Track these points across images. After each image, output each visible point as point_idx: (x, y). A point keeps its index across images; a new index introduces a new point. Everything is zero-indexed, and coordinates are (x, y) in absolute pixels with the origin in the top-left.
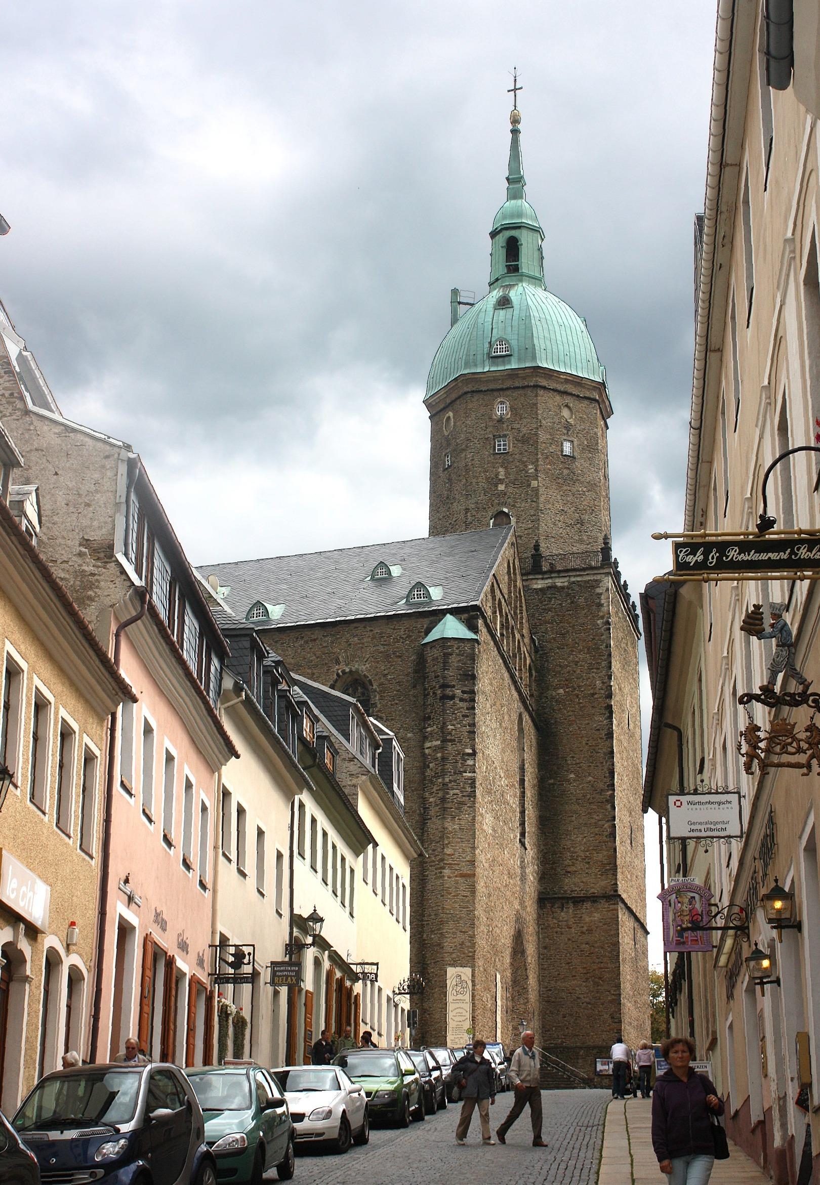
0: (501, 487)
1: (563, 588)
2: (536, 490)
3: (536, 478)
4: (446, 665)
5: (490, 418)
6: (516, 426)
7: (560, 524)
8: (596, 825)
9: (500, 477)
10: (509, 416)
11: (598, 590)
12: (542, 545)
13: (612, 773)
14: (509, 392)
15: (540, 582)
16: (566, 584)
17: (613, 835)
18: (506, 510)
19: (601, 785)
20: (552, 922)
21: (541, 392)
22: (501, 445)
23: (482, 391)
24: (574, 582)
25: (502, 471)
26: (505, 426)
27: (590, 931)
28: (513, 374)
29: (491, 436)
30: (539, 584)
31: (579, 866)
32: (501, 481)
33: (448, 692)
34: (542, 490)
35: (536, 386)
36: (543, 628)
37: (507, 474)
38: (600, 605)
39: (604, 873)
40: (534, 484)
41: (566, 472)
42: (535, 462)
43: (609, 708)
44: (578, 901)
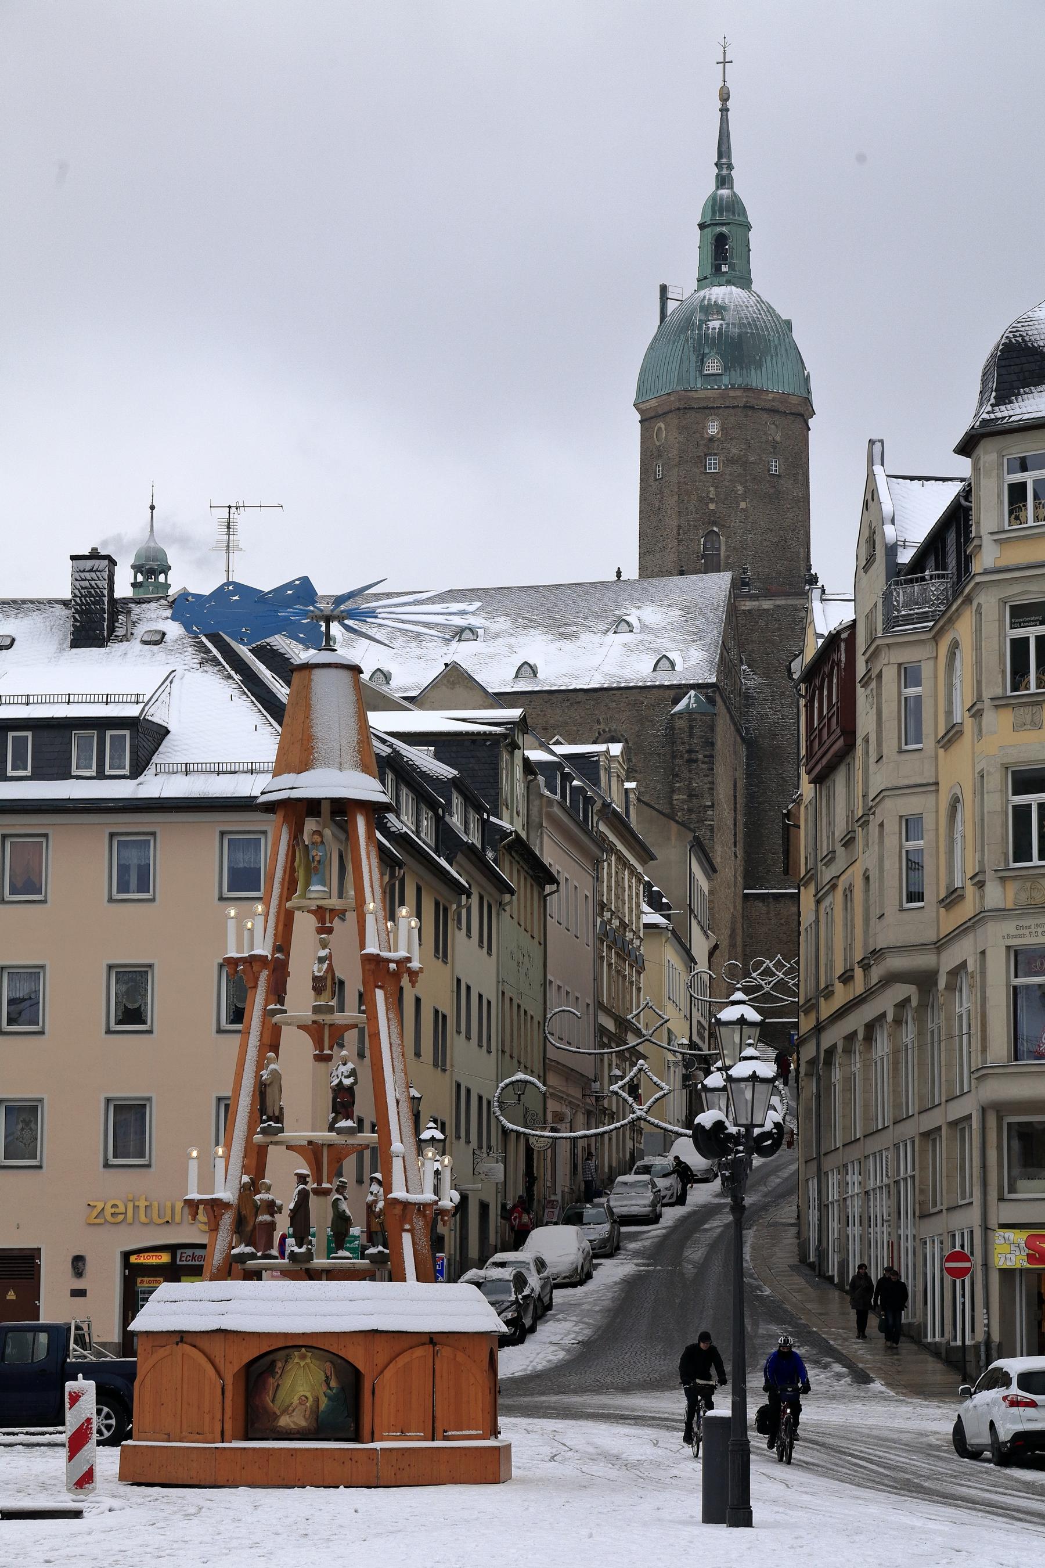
1: (768, 610)
4: (691, 735)
7: (765, 543)
9: (711, 496)
10: (720, 436)
14: (721, 411)
15: (747, 603)
16: (772, 607)
18: (715, 529)
22: (713, 466)
23: (693, 408)
24: (779, 606)
26: (715, 445)
29: (702, 454)
32: (712, 500)
33: (693, 756)
36: (750, 647)
40: (743, 505)
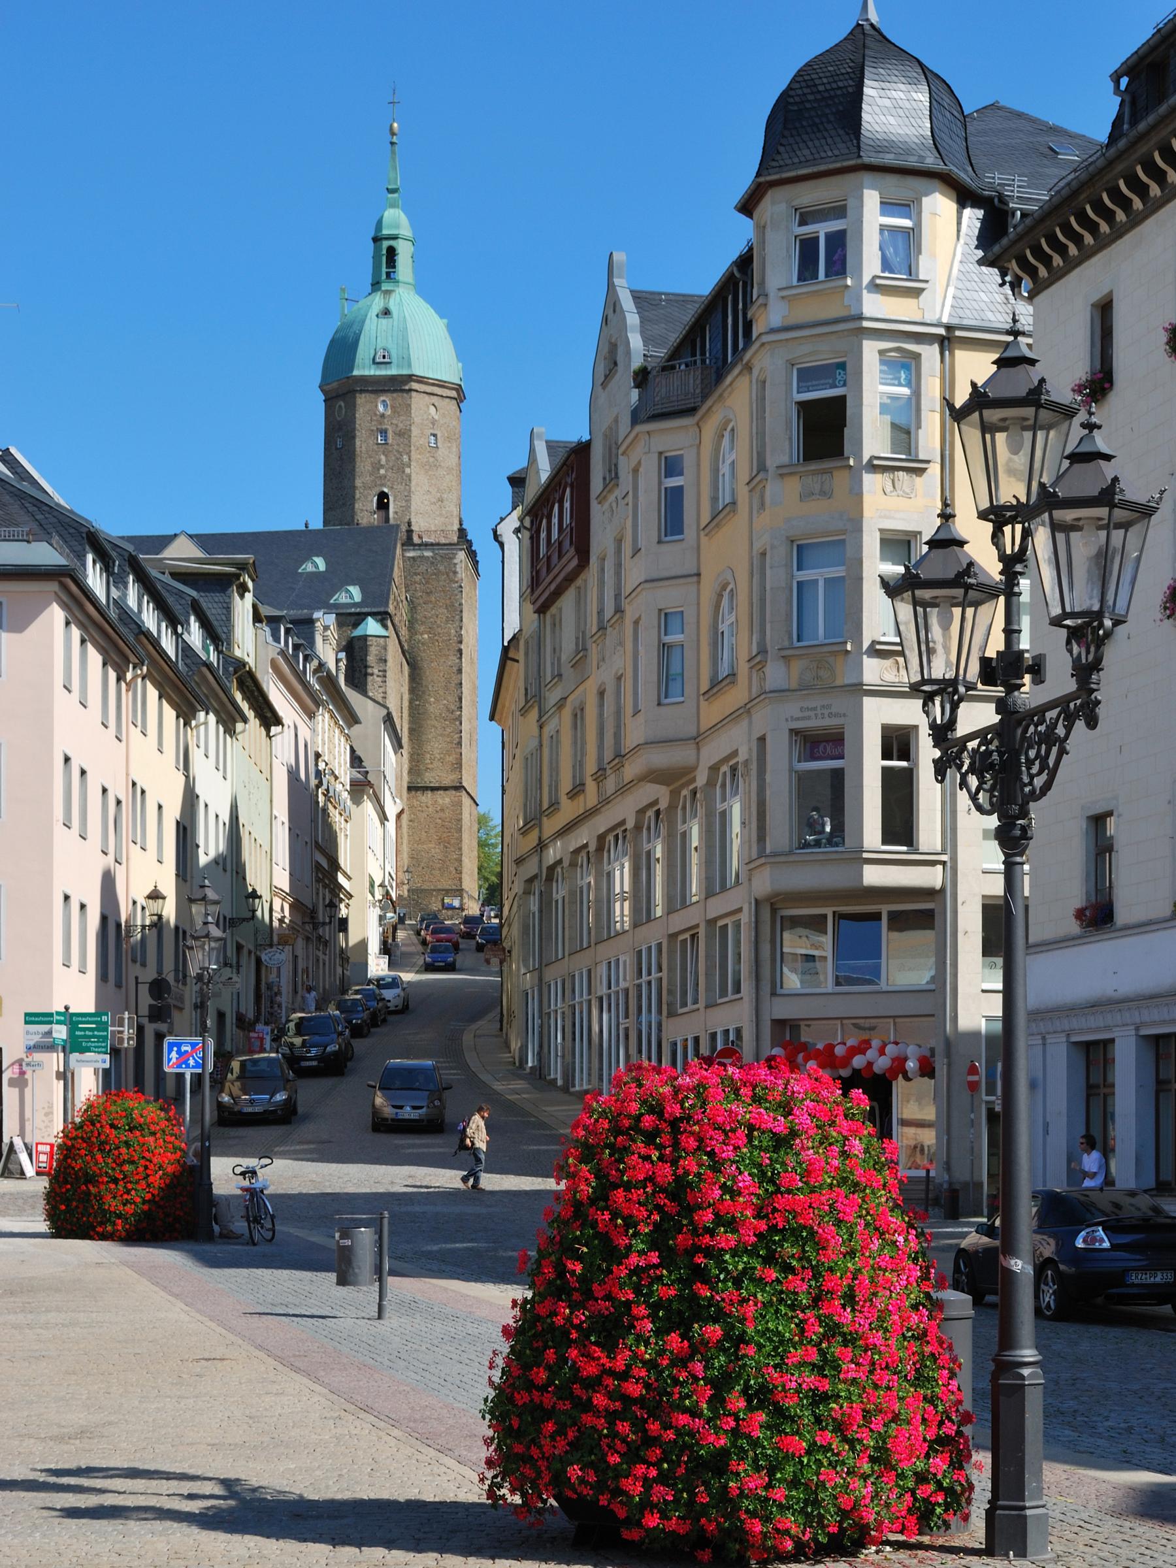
0: (382, 472)
2: (409, 476)
3: (409, 466)
5: (376, 415)
6: (395, 422)
8: (448, 736)
11: (455, 561)
12: (413, 521)
13: (460, 699)
17: (460, 744)
19: (453, 707)
20: (416, 803)
21: (414, 394)
25: (383, 458)
27: (442, 810)
28: (393, 379)
30: (411, 554)
31: (436, 764)
32: (382, 466)
34: (413, 476)
35: (410, 390)
37: (387, 461)
38: (455, 573)
39: (453, 770)
41: (431, 460)
42: (409, 454)
43: (460, 651)
44: (433, 789)
